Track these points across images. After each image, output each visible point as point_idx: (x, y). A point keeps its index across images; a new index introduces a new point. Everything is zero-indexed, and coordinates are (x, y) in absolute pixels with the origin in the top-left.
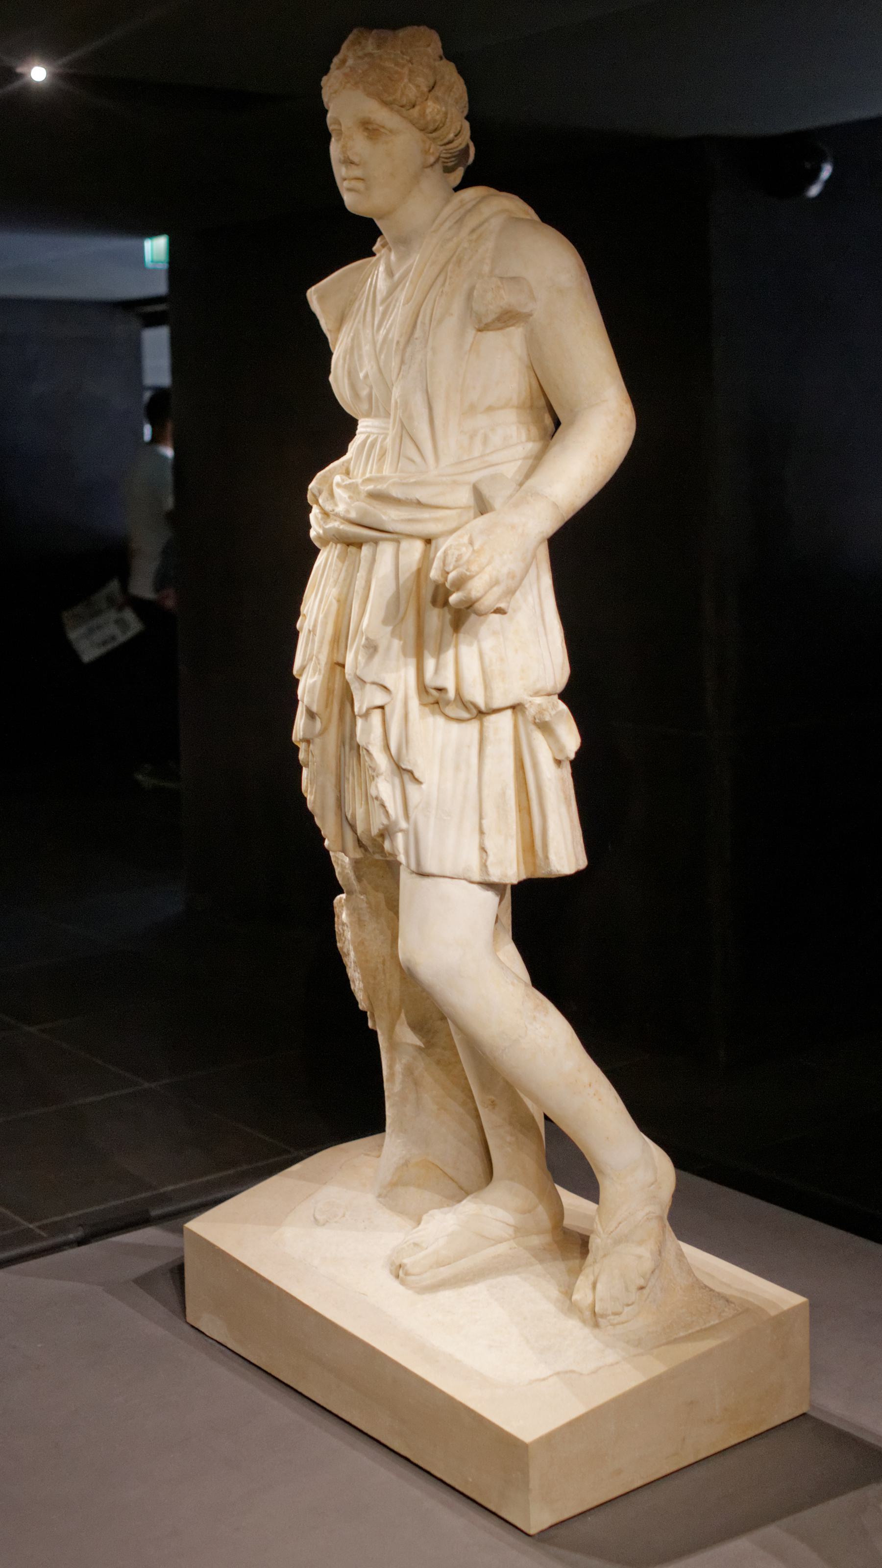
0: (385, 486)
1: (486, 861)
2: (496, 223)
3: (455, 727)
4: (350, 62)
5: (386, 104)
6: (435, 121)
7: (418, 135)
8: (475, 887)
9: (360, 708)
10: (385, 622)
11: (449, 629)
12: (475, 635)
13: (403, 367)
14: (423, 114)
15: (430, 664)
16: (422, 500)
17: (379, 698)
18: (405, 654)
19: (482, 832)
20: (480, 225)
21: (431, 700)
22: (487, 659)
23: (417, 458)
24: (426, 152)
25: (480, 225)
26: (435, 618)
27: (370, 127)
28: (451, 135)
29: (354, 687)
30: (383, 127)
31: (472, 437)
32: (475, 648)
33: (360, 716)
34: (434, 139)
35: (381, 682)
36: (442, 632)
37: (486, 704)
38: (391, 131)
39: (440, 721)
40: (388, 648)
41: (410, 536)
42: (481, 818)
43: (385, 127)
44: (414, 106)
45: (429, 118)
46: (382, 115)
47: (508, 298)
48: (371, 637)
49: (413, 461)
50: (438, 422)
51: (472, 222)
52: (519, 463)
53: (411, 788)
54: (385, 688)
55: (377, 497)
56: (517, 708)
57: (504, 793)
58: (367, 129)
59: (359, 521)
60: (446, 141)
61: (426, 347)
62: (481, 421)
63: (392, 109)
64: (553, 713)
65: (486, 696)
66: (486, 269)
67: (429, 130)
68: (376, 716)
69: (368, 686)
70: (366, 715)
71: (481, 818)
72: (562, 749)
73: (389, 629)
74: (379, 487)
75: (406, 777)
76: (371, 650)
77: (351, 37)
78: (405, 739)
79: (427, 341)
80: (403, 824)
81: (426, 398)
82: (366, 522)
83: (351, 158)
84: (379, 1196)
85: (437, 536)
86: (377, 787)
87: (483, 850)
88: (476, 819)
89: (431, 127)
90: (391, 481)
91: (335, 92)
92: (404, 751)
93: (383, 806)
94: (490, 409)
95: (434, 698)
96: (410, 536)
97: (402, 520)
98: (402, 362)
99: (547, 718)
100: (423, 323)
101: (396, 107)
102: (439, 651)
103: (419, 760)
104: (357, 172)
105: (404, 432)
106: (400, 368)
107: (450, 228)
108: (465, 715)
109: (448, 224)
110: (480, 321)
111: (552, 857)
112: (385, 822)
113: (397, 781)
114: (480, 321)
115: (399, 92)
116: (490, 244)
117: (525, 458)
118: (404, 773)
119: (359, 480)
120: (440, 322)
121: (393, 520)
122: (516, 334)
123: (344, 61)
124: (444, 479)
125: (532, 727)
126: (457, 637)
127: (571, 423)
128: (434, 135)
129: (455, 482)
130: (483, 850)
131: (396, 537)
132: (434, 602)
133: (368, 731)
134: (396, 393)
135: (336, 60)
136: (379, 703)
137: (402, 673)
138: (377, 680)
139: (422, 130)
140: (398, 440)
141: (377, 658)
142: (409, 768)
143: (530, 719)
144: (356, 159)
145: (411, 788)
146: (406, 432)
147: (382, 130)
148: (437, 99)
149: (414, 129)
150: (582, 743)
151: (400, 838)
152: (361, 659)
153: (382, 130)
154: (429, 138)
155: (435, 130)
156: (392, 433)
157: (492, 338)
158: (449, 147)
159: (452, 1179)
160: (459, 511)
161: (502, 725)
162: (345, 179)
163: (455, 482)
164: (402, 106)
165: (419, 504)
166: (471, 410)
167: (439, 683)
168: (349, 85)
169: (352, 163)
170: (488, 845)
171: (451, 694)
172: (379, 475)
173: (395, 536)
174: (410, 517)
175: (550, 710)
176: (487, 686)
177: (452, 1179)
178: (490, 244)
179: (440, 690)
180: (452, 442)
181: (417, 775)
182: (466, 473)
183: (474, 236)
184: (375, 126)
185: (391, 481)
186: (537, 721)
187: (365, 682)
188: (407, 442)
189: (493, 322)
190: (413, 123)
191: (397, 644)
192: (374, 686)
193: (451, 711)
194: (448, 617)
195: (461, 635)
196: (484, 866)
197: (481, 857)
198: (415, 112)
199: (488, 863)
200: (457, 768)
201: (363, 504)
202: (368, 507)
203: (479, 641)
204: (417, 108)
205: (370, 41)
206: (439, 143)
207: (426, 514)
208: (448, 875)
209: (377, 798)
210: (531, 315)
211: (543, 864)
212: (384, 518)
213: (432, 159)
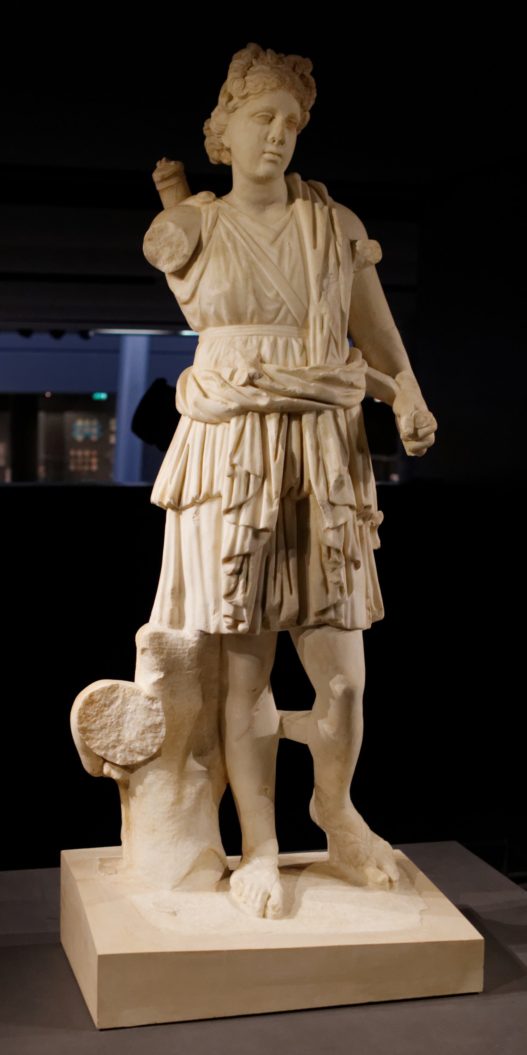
13: (323, 293)
16: (355, 383)
27: (294, 120)
43: (253, 118)
58: (290, 122)
61: (338, 280)
74: (331, 373)
75: (352, 566)
80: (347, 599)
82: (323, 397)
104: (281, 150)
168: (283, 87)
174: (348, 394)
187: (333, 504)
205: (269, 57)
209: (337, 583)
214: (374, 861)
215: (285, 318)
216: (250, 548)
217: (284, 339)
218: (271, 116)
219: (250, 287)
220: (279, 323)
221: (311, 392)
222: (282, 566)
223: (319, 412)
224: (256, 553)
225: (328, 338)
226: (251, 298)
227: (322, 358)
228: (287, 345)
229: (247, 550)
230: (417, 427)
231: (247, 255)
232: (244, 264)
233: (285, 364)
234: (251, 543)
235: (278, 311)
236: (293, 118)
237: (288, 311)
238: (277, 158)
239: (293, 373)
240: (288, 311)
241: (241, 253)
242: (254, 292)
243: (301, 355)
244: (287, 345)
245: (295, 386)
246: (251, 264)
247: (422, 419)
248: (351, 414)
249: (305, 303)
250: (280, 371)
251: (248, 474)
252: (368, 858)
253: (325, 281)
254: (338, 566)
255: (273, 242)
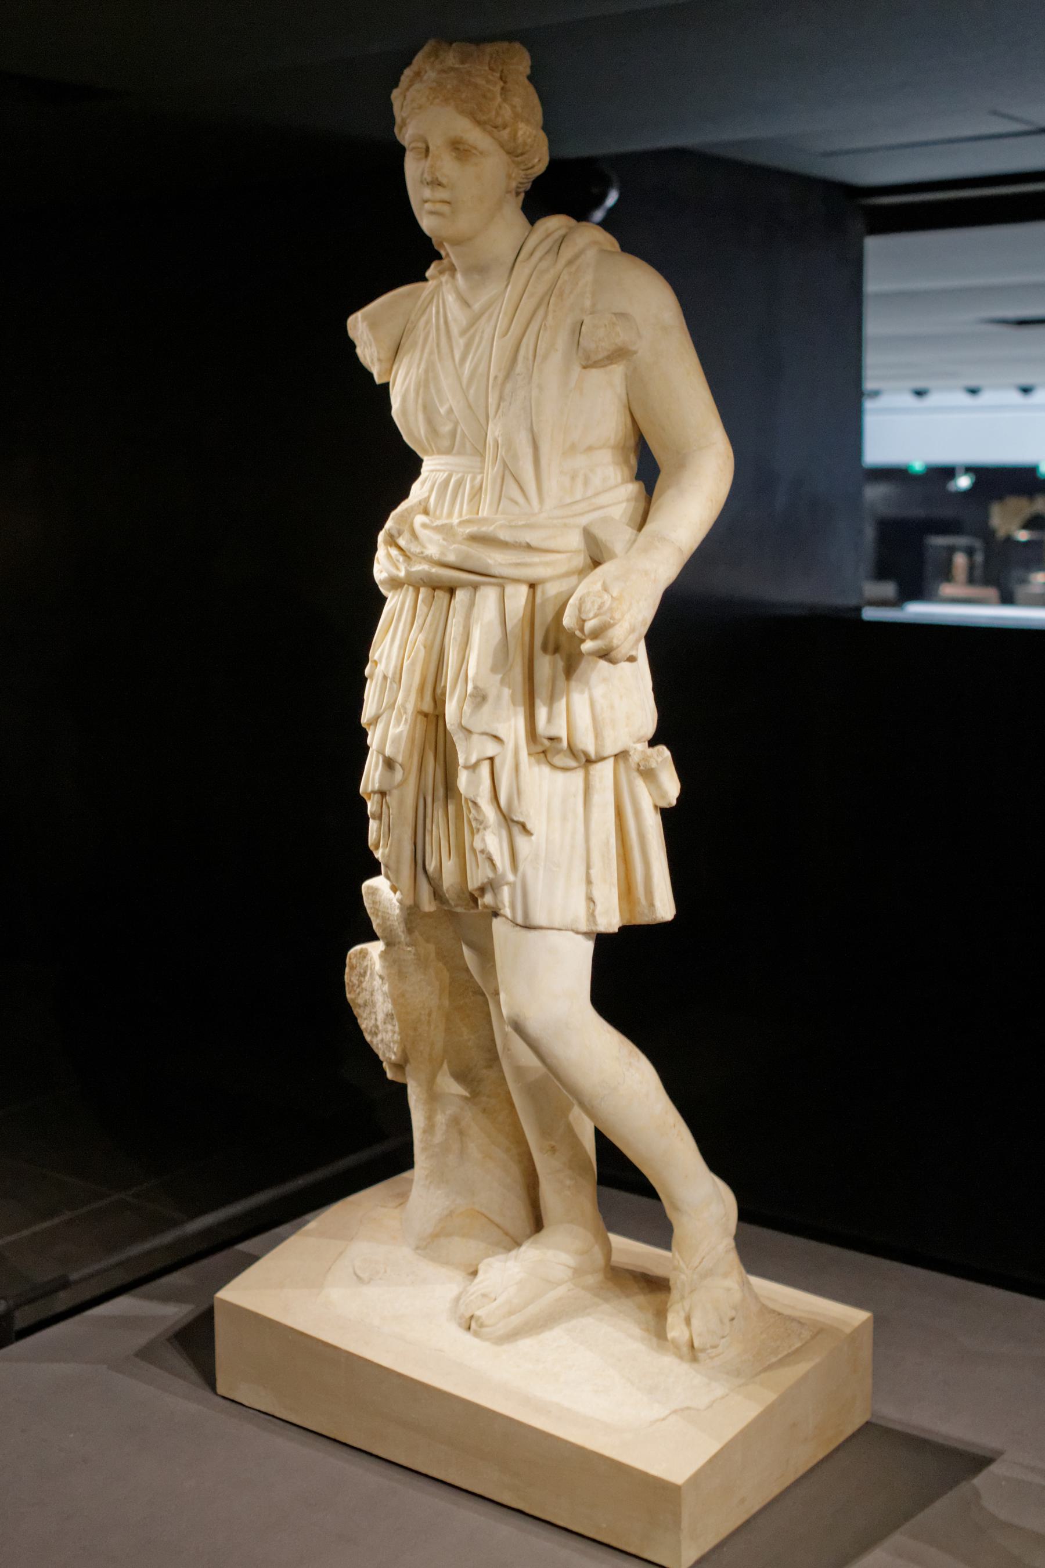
0: (491, 528)
1: (594, 911)
2: (591, 254)
3: (560, 776)
4: (431, 75)
5: (479, 123)
6: (525, 144)
7: (505, 157)
8: (580, 937)
9: (467, 759)
10: (494, 670)
11: (561, 676)
12: (587, 683)
13: (502, 404)
14: (514, 137)
15: (542, 713)
16: (533, 543)
17: (491, 749)
18: (514, 703)
19: (589, 882)
20: (576, 257)
21: (540, 749)
22: (598, 707)
23: (520, 499)
24: (509, 176)
25: (576, 257)
26: (545, 665)
27: (461, 147)
28: (536, 160)
29: (458, 739)
30: (475, 148)
31: (573, 478)
32: (586, 695)
33: (466, 767)
34: (518, 164)
35: (494, 733)
36: (554, 680)
37: (596, 752)
38: (481, 153)
39: (546, 770)
40: (499, 697)
41: (517, 581)
42: (588, 867)
43: (460, 145)
44: (505, 128)
45: (520, 140)
46: (474, 136)
47: (622, 336)
48: (480, 685)
49: (516, 503)
50: (544, 461)
51: (567, 253)
52: (624, 505)
53: (521, 841)
54: (496, 738)
55: (477, 539)
56: (622, 756)
57: (608, 842)
58: (458, 149)
59: (458, 565)
60: (530, 165)
61: (529, 383)
62: (580, 461)
63: (485, 130)
64: (660, 760)
65: (596, 744)
66: (588, 303)
67: (514, 152)
68: (485, 769)
69: (475, 738)
70: (474, 767)
71: (588, 867)
72: (664, 795)
73: (499, 677)
74: (484, 529)
75: (516, 830)
76: (479, 699)
77: (427, 48)
78: (518, 791)
79: (531, 377)
80: (511, 877)
81: (530, 437)
83: (440, 179)
84: (417, 1248)
85: (543, 581)
86: (483, 840)
87: (590, 899)
88: (583, 869)
89: (519, 151)
90: (498, 523)
91: (420, 107)
92: (516, 802)
93: (490, 859)
94: (590, 449)
95: (544, 748)
96: (517, 581)
97: (510, 564)
98: (501, 398)
99: (654, 765)
100: (526, 358)
101: (489, 128)
102: (552, 700)
103: (533, 811)
105: (507, 473)
106: (499, 405)
107: (541, 259)
108: (573, 763)
109: (538, 254)
110: (588, 358)
111: (658, 903)
112: (491, 875)
113: (504, 834)
114: (588, 358)
115: (494, 113)
116: (588, 277)
117: (628, 500)
118: (513, 824)
119: (455, 520)
120: (545, 357)
121: (500, 564)
122: (617, 372)
123: (418, 74)
124: (555, 521)
125: (635, 774)
126: (568, 685)
127: (681, 464)
128: (519, 159)
129: (565, 525)
130: (590, 899)
131: (501, 582)
132: (545, 649)
133: (474, 783)
134: (495, 431)
135: (408, 72)
136: (490, 754)
137: (512, 722)
138: (488, 731)
139: (508, 153)
140: (499, 480)
141: (486, 708)
142: (521, 820)
143: (634, 766)
144: (444, 181)
145: (521, 841)
146: (509, 472)
147: (474, 151)
148: (527, 121)
149: (502, 152)
150: (681, 790)
151: (506, 891)
152: (467, 708)
153: (474, 151)
154: (513, 162)
155: (522, 154)
156: (491, 471)
157: (594, 373)
158: (529, 172)
159: (498, 1226)
160: (568, 555)
161: (604, 772)
162: (426, 202)
163: (565, 525)
164: (496, 127)
165: (529, 547)
166: (572, 450)
167: (553, 733)
168: (437, 101)
169: (440, 184)
170: (596, 894)
171: (565, 744)
172: (475, 516)
173: (500, 581)
174: (519, 561)
175: (655, 756)
176: (598, 735)
177: (498, 1226)
178: (588, 277)
179: (551, 739)
180: (553, 483)
181: (529, 826)
182: (575, 515)
183: (573, 268)
184: (466, 147)
185: (498, 523)
186: (642, 768)
187: (469, 732)
188: (509, 480)
189: (600, 360)
190: (502, 146)
191: (506, 692)
192: (485, 737)
193: (558, 760)
194: (561, 664)
195: (573, 683)
196: (592, 916)
197: (588, 908)
198: (505, 134)
199: (597, 913)
200: (564, 818)
201: (463, 547)
202: (470, 550)
203: (590, 689)
204: (508, 130)
205: (451, 54)
206: (523, 167)
207: (536, 558)
208: (557, 925)
209: (482, 852)
210: (635, 352)
211: (646, 911)
212: (490, 561)
213: (514, 184)
214: (687, 1308)
215: (463, 445)
216: (380, 782)
217: (460, 475)
218: (424, 146)
219: (420, 401)
220: (459, 453)
221: (451, 558)
222: (440, 814)
223: (475, 587)
224: (395, 792)
225: (501, 474)
226: (421, 417)
227: (490, 505)
228: (460, 483)
229: (377, 786)
230: (584, 617)
231: (431, 353)
232: (423, 366)
233: (450, 514)
234: (381, 775)
235: (453, 434)
236: (458, 142)
237: (464, 436)
238: (439, 207)
239: (438, 529)
240: (464, 436)
241: (427, 351)
242: (425, 407)
243: (471, 500)
244: (460, 483)
245: (432, 551)
246: (430, 368)
247: (588, 605)
248: (543, 592)
249: (483, 421)
250: (424, 526)
251: (385, 678)
252: (683, 1298)
253: (509, 386)
254: (481, 827)
255: (463, 332)
